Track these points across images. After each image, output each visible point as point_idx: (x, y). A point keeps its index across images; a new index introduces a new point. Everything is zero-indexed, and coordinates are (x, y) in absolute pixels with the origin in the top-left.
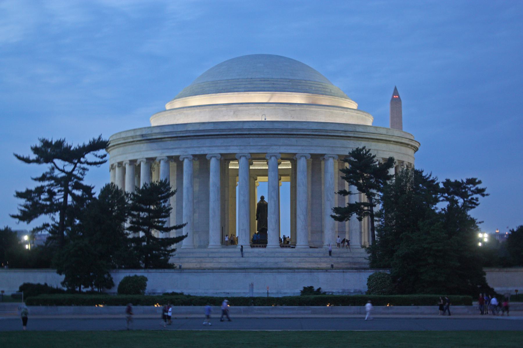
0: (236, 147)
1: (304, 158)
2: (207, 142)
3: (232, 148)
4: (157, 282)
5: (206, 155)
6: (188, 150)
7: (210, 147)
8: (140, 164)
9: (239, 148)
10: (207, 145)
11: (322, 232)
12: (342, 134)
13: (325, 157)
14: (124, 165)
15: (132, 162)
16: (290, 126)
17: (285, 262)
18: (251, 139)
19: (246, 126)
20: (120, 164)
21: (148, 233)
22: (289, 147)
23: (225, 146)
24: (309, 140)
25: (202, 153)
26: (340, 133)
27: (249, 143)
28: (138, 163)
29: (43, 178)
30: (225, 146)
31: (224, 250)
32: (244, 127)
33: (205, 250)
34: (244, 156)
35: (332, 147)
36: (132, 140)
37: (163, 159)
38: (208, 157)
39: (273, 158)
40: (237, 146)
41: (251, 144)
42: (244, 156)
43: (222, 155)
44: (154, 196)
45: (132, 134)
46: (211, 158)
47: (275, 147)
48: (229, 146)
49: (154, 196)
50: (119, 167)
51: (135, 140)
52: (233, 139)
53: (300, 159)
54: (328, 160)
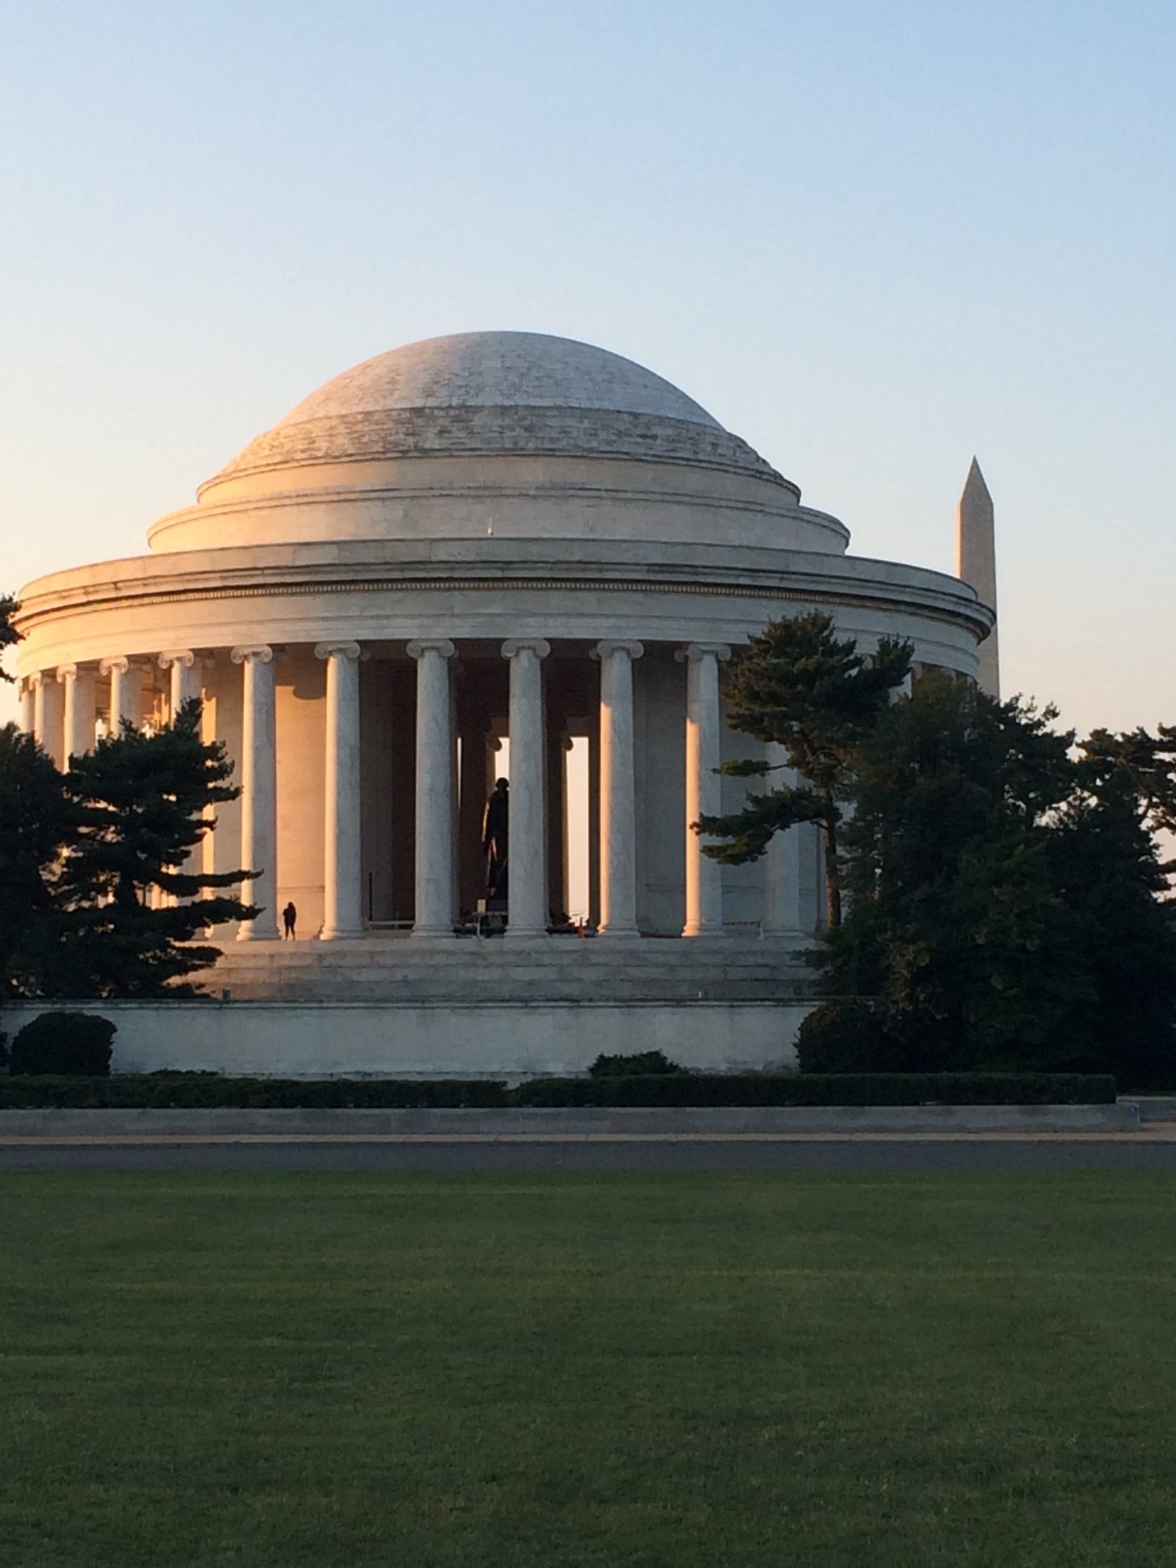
0: (409, 622)
1: (624, 654)
3: (398, 622)
4: (147, 1037)
8: (110, 673)
9: (418, 621)
12: (742, 581)
14: (59, 680)
15: (89, 670)
19: (441, 553)
21: (125, 895)
22: (573, 621)
23: (372, 617)
24: (639, 597)
26: (738, 576)
27: (452, 607)
28: (104, 672)
30: (372, 617)
31: (368, 945)
32: (434, 559)
34: (433, 648)
36: (84, 599)
37: (179, 659)
38: (319, 653)
39: (524, 654)
40: (412, 617)
41: (456, 611)
42: (433, 648)
43: (363, 644)
45: (86, 579)
47: (532, 621)
48: (387, 617)
51: (92, 598)
52: (400, 595)
53: (610, 656)
54: (700, 660)
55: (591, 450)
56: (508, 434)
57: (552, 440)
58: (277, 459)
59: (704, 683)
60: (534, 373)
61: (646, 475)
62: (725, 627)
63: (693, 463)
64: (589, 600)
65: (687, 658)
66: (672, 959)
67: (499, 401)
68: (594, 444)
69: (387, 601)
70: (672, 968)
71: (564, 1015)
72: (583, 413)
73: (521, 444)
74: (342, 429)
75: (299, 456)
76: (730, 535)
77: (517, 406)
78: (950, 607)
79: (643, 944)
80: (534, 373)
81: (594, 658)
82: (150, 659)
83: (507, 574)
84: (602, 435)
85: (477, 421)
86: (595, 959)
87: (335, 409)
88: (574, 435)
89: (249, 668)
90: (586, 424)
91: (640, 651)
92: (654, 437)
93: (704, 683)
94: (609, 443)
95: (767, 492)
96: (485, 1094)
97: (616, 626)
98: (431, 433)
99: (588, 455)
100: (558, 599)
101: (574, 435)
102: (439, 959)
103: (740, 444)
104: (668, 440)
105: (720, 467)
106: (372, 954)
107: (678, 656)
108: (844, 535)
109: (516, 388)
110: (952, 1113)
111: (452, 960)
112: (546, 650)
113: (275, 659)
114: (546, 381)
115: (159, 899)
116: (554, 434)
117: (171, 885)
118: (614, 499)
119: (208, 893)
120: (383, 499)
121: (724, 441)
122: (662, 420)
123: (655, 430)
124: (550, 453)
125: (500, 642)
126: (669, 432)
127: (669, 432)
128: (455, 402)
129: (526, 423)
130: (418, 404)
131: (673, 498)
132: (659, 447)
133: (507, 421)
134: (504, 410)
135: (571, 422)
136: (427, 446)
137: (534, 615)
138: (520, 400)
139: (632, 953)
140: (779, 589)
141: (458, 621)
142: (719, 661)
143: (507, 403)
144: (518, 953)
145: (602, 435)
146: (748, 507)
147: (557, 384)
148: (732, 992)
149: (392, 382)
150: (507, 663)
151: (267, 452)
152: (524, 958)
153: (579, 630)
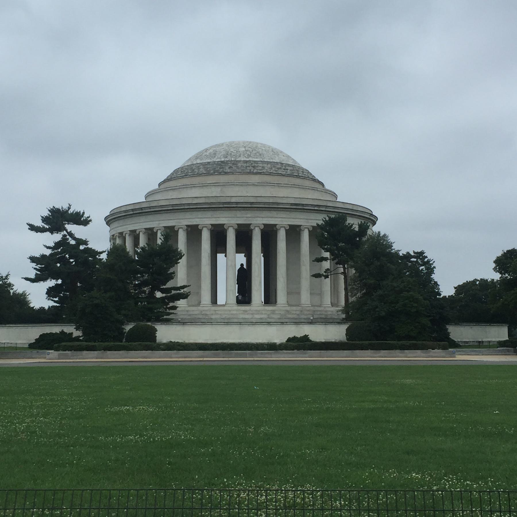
2: (200, 214)
4: (164, 333)
5: (198, 225)
6: (182, 221)
7: (201, 218)
9: (227, 219)
10: (199, 216)
11: (299, 293)
12: (316, 208)
13: (302, 227)
16: (271, 201)
17: (268, 318)
18: (238, 211)
19: (234, 200)
20: (121, 234)
25: (195, 223)
28: (137, 232)
29: (58, 245)
33: (199, 308)
35: (307, 219)
36: (132, 213)
37: (160, 229)
38: (200, 227)
40: (226, 217)
43: (212, 225)
44: (159, 259)
46: (203, 227)
47: (259, 219)
48: (219, 217)
49: (159, 259)
50: (119, 237)
51: (134, 212)
55: (271, 173)
56: (248, 168)
57: (260, 170)
58: (184, 175)
59: (305, 236)
60: (254, 152)
61: (285, 180)
62: (310, 221)
63: (298, 177)
64: (274, 213)
65: (300, 230)
66: (298, 313)
67: (245, 159)
68: (272, 171)
69: (218, 213)
70: (298, 314)
71: (279, 327)
72: (268, 163)
73: (252, 171)
74: (201, 167)
75: (189, 174)
76: (309, 196)
77: (250, 161)
78: (368, 217)
79: (288, 308)
80: (254, 152)
81: (275, 229)
82: (151, 229)
83: (252, 206)
84: (274, 169)
85: (239, 165)
86: (277, 312)
87: (199, 161)
88: (266, 168)
89: (181, 231)
90: (269, 166)
91: (288, 228)
92: (287, 169)
93: (305, 236)
94: (276, 171)
95: (317, 185)
96: (272, 347)
97: (282, 221)
98: (227, 168)
99: (270, 174)
100: (266, 213)
101: (266, 168)
102: (235, 312)
103: (309, 172)
104: (291, 170)
105: (304, 178)
106: (215, 311)
107: (298, 229)
108: (335, 196)
109: (249, 156)
110: (416, 352)
111: (238, 313)
112: (262, 227)
113: (187, 229)
114: (258, 154)
115: (159, 295)
116: (260, 168)
117: (163, 291)
118: (279, 186)
119: (173, 292)
120: (215, 186)
121: (305, 171)
122: (289, 165)
123: (287, 168)
124: (260, 173)
125: (250, 225)
126: (291, 168)
127: (291, 168)
128: (233, 159)
129: (253, 165)
130: (223, 160)
131: (294, 186)
132: (289, 172)
133: (248, 165)
134: (246, 162)
135: (265, 165)
136: (226, 171)
137: (259, 217)
138: (250, 159)
139: (288, 311)
140: (325, 211)
141: (238, 219)
142: (309, 231)
143: (247, 160)
144: (256, 310)
145: (274, 169)
146: (313, 189)
147: (260, 155)
148: (326, 321)
149: (215, 154)
150: (251, 231)
151: (180, 173)
152: (258, 312)
153: (272, 222)
